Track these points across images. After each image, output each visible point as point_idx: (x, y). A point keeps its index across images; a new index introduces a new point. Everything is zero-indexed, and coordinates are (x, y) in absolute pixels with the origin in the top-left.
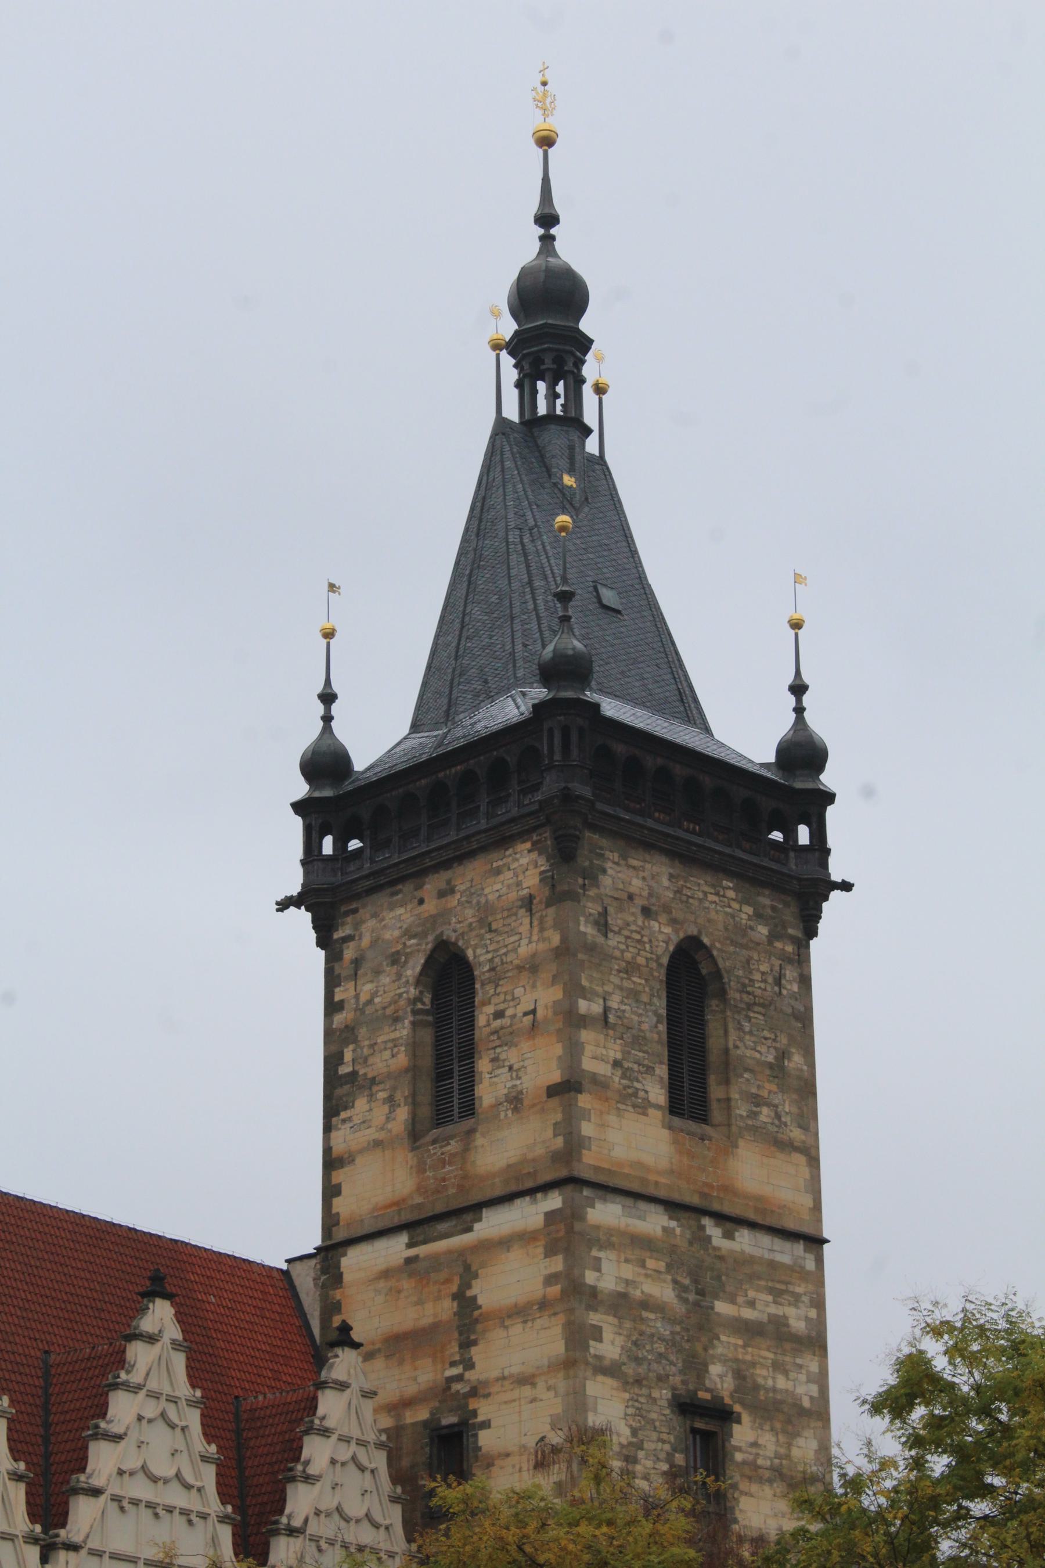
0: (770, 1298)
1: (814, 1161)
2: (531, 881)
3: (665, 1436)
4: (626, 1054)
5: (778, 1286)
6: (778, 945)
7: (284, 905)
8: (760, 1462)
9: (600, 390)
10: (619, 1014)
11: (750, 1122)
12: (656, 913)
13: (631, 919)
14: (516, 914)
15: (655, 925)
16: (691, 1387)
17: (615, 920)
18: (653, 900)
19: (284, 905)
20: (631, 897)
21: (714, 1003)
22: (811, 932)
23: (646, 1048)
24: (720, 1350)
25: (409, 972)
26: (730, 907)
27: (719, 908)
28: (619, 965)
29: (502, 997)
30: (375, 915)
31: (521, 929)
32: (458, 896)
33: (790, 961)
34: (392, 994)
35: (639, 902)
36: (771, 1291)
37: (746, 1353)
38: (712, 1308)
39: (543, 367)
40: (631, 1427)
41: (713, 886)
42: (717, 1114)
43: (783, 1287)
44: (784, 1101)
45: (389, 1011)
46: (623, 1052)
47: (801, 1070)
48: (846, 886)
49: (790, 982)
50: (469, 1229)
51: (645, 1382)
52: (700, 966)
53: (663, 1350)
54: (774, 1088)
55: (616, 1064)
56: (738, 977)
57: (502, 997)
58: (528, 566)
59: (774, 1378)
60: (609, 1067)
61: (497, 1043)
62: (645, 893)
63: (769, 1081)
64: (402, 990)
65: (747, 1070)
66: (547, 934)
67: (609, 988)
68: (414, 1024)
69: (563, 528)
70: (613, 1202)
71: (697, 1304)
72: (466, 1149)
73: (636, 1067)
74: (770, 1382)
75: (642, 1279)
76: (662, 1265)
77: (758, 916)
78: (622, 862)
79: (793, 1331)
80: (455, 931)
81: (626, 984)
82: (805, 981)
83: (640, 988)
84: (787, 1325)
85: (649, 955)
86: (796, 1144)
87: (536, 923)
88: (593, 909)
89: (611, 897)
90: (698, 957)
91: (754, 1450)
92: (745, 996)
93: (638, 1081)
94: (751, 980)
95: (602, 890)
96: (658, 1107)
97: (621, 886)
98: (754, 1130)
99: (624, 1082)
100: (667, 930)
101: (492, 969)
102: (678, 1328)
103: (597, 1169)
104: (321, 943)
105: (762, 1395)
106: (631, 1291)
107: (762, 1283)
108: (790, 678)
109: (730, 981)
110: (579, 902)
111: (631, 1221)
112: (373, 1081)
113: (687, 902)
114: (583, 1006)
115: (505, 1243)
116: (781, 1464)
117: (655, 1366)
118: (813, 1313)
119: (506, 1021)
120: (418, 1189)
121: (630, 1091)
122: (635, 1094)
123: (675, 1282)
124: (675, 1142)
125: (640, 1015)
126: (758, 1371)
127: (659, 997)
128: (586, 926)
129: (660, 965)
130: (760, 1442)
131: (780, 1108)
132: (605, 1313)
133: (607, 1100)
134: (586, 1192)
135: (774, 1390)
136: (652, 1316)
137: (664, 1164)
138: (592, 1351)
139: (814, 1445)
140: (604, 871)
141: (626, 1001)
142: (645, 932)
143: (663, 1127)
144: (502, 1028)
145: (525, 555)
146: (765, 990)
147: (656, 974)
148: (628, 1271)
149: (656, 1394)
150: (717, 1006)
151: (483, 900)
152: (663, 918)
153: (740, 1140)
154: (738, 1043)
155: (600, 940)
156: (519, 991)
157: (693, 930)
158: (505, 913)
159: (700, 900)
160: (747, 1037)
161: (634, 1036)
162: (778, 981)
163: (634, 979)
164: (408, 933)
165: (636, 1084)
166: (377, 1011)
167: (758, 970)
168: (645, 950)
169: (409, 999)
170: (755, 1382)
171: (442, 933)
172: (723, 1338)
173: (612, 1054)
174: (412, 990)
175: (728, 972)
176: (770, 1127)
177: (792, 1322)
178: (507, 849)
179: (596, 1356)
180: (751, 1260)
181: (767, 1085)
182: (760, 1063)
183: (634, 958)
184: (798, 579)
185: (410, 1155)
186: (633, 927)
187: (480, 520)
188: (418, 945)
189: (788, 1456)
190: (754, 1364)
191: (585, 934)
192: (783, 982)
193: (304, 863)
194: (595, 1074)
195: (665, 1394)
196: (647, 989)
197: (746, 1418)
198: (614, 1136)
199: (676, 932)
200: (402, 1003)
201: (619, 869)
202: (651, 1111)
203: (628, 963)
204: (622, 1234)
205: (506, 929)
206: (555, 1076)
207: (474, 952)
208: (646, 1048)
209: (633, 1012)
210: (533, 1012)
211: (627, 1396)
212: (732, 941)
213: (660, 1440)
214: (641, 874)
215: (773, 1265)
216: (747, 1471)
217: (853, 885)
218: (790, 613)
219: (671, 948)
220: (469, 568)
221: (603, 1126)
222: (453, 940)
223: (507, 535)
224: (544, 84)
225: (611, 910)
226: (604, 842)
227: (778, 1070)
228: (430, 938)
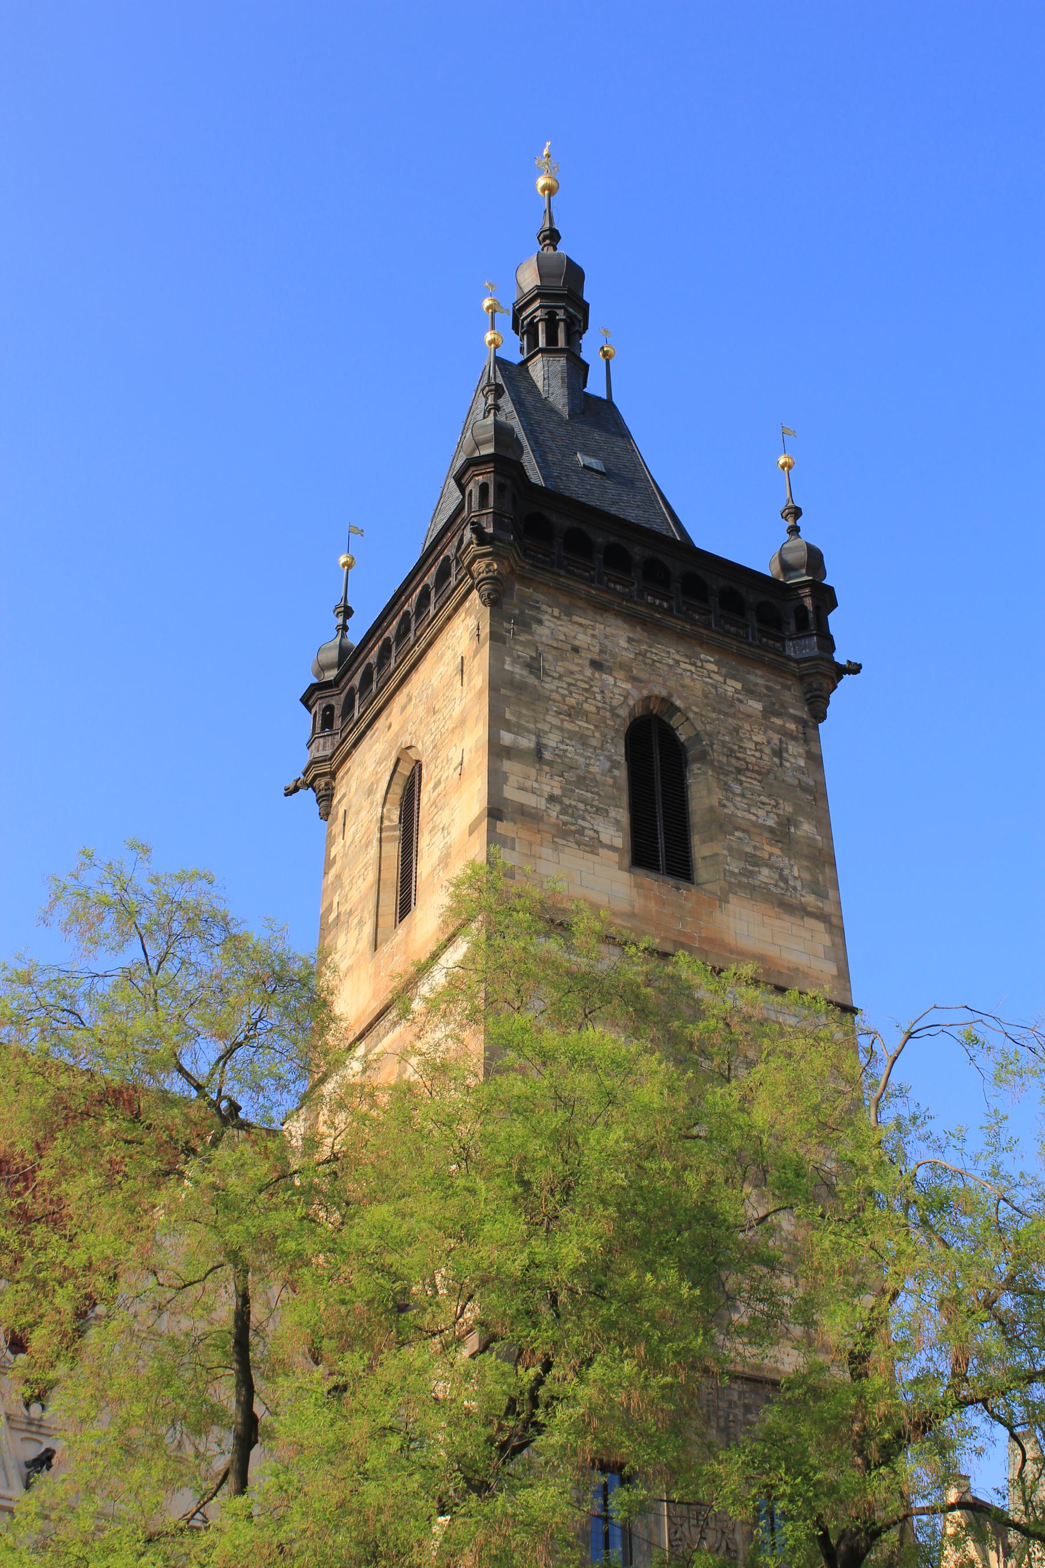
1: (836, 928)
4: (567, 792)
6: (778, 721)
10: (557, 752)
11: (744, 880)
13: (575, 668)
17: (549, 661)
18: (606, 657)
20: (576, 650)
21: (695, 768)
22: (821, 716)
23: (596, 790)
27: (695, 676)
28: (558, 707)
33: (794, 738)
41: (687, 656)
42: (702, 871)
44: (792, 866)
47: (814, 839)
52: (678, 733)
54: (777, 851)
55: (552, 799)
56: (723, 742)
60: (543, 801)
62: (597, 649)
65: (737, 829)
73: (581, 806)
81: (566, 725)
82: (816, 760)
83: (589, 733)
85: (600, 705)
86: (809, 909)
88: (526, 653)
90: (674, 722)
92: (734, 761)
93: (584, 819)
94: (740, 747)
96: (612, 848)
100: (627, 686)
109: (711, 745)
110: (504, 643)
121: (573, 828)
122: (581, 831)
125: (589, 758)
128: (513, 666)
133: (539, 831)
137: (624, 906)
140: (540, 622)
141: (568, 741)
150: (699, 769)
152: (620, 674)
153: (730, 895)
154: (725, 802)
155: (532, 680)
159: (670, 666)
160: (739, 799)
161: (579, 777)
162: (779, 753)
163: (580, 723)
167: (751, 739)
168: (595, 699)
173: (547, 789)
175: (710, 735)
176: (772, 888)
181: (767, 847)
182: (754, 824)
192: (785, 755)
194: (522, 805)
201: (559, 623)
202: (601, 851)
208: (596, 790)
209: (576, 753)
217: (860, 666)
226: (540, 597)
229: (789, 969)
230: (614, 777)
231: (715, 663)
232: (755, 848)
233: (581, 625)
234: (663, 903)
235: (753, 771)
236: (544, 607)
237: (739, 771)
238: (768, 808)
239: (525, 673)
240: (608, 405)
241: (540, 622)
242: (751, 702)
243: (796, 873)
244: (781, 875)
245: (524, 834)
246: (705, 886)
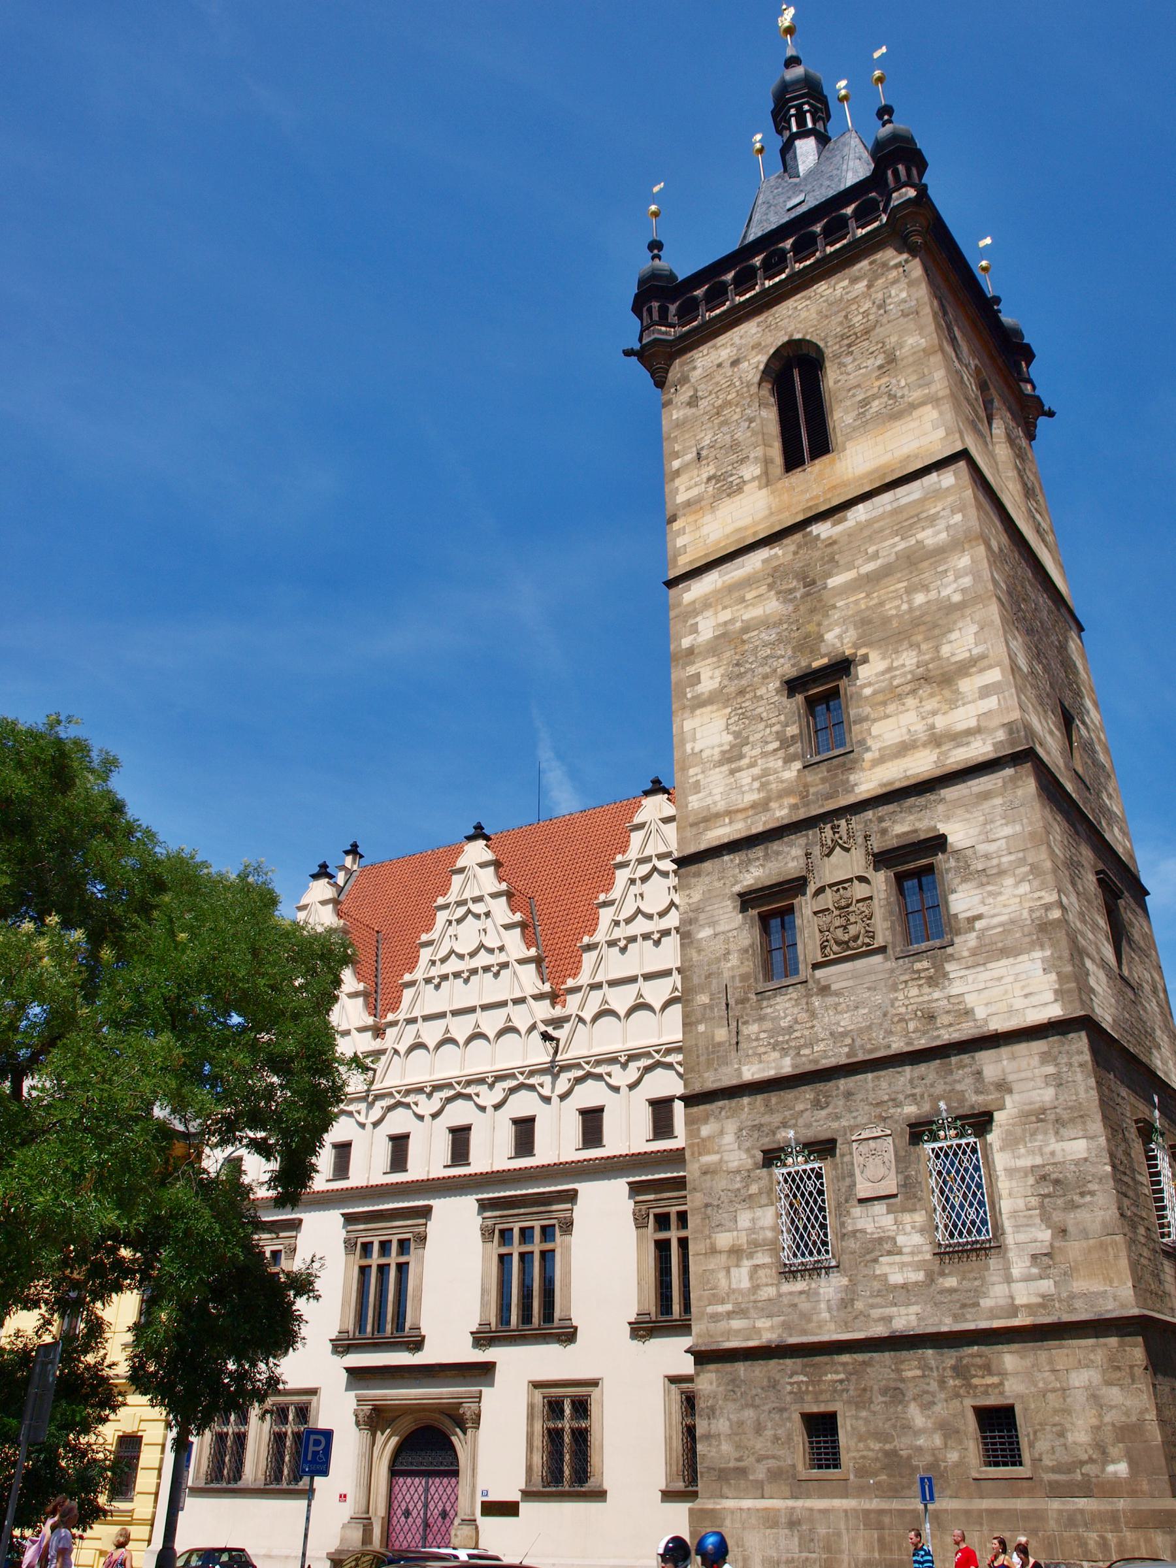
0: (897, 539)
3: (773, 721)
4: (718, 468)
8: (895, 683)
16: (803, 664)
20: (719, 365)
24: (836, 615)
33: (895, 281)
35: (727, 364)
37: (872, 599)
38: (825, 588)
53: (769, 652)
55: (709, 479)
59: (909, 602)
63: (878, 378)
65: (849, 390)
71: (808, 594)
74: (905, 607)
79: (931, 548)
84: (924, 547)
90: (805, 351)
91: (888, 676)
93: (732, 475)
95: (693, 380)
102: (785, 626)
103: (691, 562)
105: (895, 624)
106: (731, 627)
107: (888, 531)
111: (726, 578)
116: (928, 670)
123: (778, 593)
126: (887, 607)
130: (895, 665)
136: (756, 633)
138: (689, 696)
139: (974, 628)
143: (760, 488)
159: (789, 316)
162: (882, 305)
165: (731, 479)
172: (838, 605)
173: (705, 476)
175: (824, 339)
176: (884, 410)
179: (693, 697)
180: (869, 523)
181: (877, 384)
182: (864, 375)
189: (939, 658)
190: (881, 604)
192: (888, 301)
195: (774, 684)
197: (874, 656)
204: (716, 592)
211: (729, 710)
213: (766, 727)
216: (880, 698)
229: (901, 462)
230: (753, 431)
237: (849, 346)
241: (695, 368)
242: (856, 287)
245: (691, 519)
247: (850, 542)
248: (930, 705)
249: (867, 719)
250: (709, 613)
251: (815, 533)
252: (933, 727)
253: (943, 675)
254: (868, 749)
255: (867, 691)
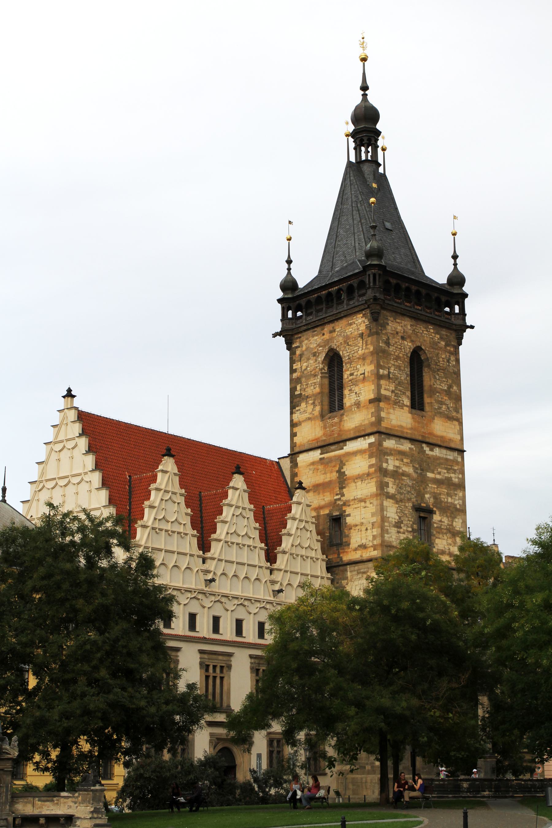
0: (446, 471)
1: (461, 424)
2: (363, 328)
3: (410, 519)
4: (396, 388)
5: (449, 467)
6: (448, 348)
7: (275, 335)
8: (442, 527)
9: (384, 150)
12: (406, 338)
14: (357, 339)
15: (406, 343)
16: (419, 502)
17: (392, 341)
19: (275, 335)
20: (397, 333)
21: (425, 370)
22: (460, 344)
25: (319, 359)
26: (431, 335)
29: (353, 368)
30: (307, 339)
31: (359, 345)
32: (337, 333)
33: (452, 354)
34: (313, 367)
35: (400, 334)
36: (446, 469)
37: (438, 490)
38: (426, 475)
39: (363, 142)
40: (398, 516)
41: (426, 328)
42: (427, 408)
43: (450, 467)
45: (312, 373)
46: (395, 387)
47: (456, 392)
48: (472, 327)
49: (452, 361)
50: (342, 449)
51: (403, 501)
54: (447, 398)
55: (393, 392)
56: (434, 360)
57: (353, 368)
58: (360, 215)
59: (447, 499)
60: (390, 393)
61: (351, 384)
62: (402, 332)
63: (446, 396)
64: (317, 365)
66: (368, 347)
67: (390, 365)
68: (321, 377)
69: (373, 203)
70: (392, 439)
71: (421, 474)
72: (341, 421)
73: (399, 392)
75: (402, 466)
76: (409, 461)
77: (441, 338)
78: (394, 321)
79: (454, 482)
80: (336, 345)
81: (396, 363)
82: (458, 361)
84: (452, 480)
85: (404, 353)
86: (455, 418)
87: (364, 342)
88: (384, 338)
89: (390, 333)
91: (440, 523)
92: (437, 366)
93: (400, 397)
94: (439, 361)
95: (387, 331)
96: (407, 406)
97: (394, 329)
98: (440, 413)
99: (395, 398)
100: (410, 344)
101: (349, 359)
103: (386, 428)
104: (289, 348)
107: (443, 466)
108: (452, 253)
109: (431, 362)
110: (379, 335)
111: (398, 446)
112: (307, 397)
113: (417, 334)
114: (381, 371)
115: (355, 453)
117: (406, 495)
118: (460, 476)
119: (354, 377)
120: (324, 434)
121: (397, 401)
122: (399, 402)
123: (413, 466)
124: (413, 418)
127: (407, 368)
129: (407, 357)
131: (449, 406)
132: (390, 478)
133: (390, 404)
134: (383, 436)
135: (447, 502)
136: (406, 478)
137: (409, 426)
138: (385, 490)
139: (461, 521)
140: (388, 324)
142: (402, 345)
144: (353, 379)
145: (358, 210)
146: (444, 364)
147: (406, 360)
148: (397, 463)
149: (407, 505)
151: (345, 334)
152: (408, 340)
155: (387, 348)
156: (358, 366)
157: (418, 344)
158: (353, 339)
162: (448, 361)
164: (319, 346)
166: (308, 372)
167: (441, 357)
169: (320, 369)
170: (441, 500)
171: (331, 346)
172: (430, 485)
173: (391, 388)
174: (321, 365)
175: (431, 358)
176: (445, 412)
177: (453, 479)
178: (354, 317)
180: (439, 458)
181: (445, 398)
182: (442, 390)
183: (399, 354)
184: (455, 217)
185: (321, 423)
186: (398, 344)
187: (342, 199)
188: (322, 350)
189: (452, 525)
190: (440, 494)
191: (382, 346)
192: (450, 361)
193: (282, 320)
195: (411, 505)
196: (403, 365)
197: (437, 513)
198: (392, 417)
199: (413, 345)
200: (317, 370)
202: (405, 408)
203: (397, 356)
204: (395, 450)
205: (354, 345)
206: (372, 396)
207: (343, 353)
209: (398, 373)
210: (364, 374)
211: (397, 506)
212: (432, 347)
213: (408, 520)
214: (401, 325)
215: (447, 460)
218: (452, 230)
219: (411, 351)
220: (339, 215)
221: (389, 413)
222: (335, 348)
223: (352, 204)
224: (363, 38)
225: (390, 338)
226: (388, 314)
227: (448, 392)
228: (327, 347)
231: (433, 329)
232: (442, 398)
233: (398, 323)
234: (419, 423)
235: (442, 369)
236: (389, 318)
238: (445, 383)
239: (385, 346)
240: (384, 176)
243: (451, 406)
244: (448, 407)
245: (386, 406)
246: (428, 413)
247: (434, 462)
248: (450, 541)
249: (434, 535)
250: (392, 458)
251: (424, 449)
252: (449, 549)
253: (453, 532)
254: (434, 547)
255: (435, 525)
